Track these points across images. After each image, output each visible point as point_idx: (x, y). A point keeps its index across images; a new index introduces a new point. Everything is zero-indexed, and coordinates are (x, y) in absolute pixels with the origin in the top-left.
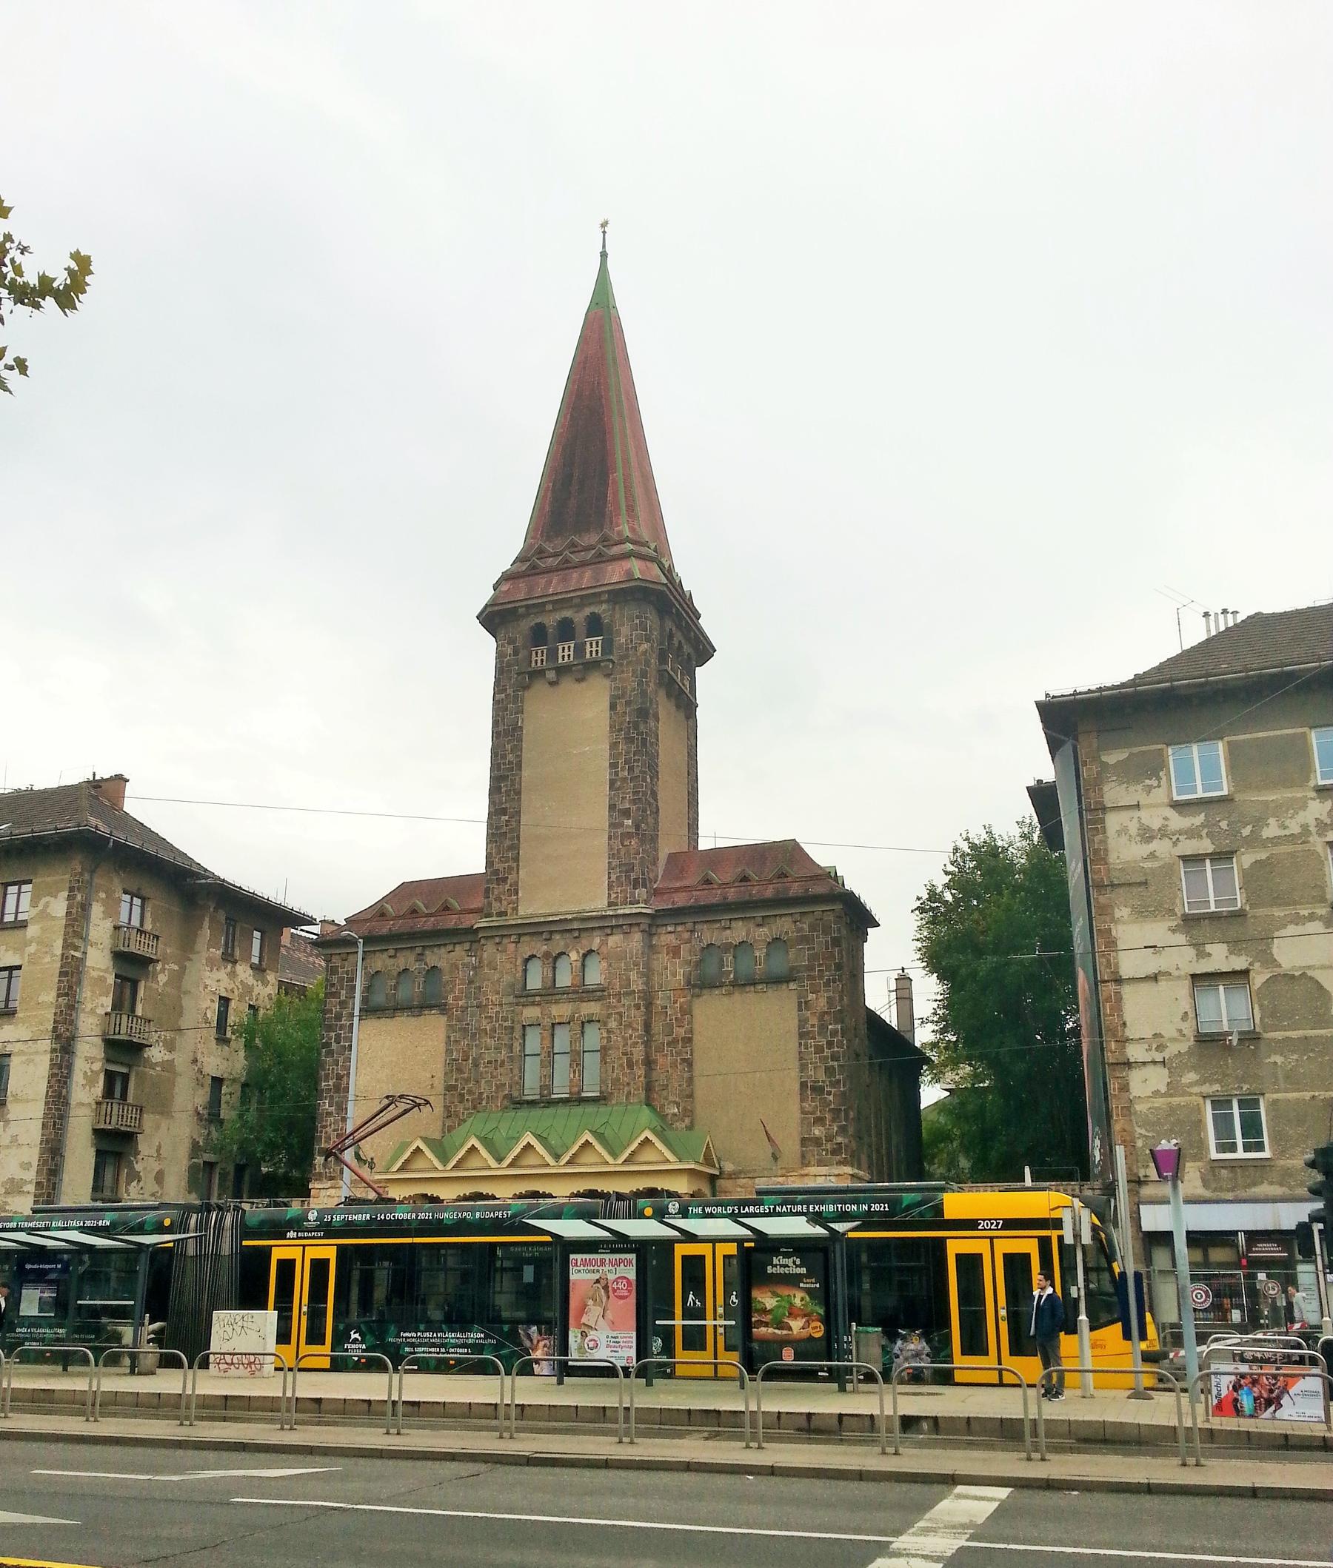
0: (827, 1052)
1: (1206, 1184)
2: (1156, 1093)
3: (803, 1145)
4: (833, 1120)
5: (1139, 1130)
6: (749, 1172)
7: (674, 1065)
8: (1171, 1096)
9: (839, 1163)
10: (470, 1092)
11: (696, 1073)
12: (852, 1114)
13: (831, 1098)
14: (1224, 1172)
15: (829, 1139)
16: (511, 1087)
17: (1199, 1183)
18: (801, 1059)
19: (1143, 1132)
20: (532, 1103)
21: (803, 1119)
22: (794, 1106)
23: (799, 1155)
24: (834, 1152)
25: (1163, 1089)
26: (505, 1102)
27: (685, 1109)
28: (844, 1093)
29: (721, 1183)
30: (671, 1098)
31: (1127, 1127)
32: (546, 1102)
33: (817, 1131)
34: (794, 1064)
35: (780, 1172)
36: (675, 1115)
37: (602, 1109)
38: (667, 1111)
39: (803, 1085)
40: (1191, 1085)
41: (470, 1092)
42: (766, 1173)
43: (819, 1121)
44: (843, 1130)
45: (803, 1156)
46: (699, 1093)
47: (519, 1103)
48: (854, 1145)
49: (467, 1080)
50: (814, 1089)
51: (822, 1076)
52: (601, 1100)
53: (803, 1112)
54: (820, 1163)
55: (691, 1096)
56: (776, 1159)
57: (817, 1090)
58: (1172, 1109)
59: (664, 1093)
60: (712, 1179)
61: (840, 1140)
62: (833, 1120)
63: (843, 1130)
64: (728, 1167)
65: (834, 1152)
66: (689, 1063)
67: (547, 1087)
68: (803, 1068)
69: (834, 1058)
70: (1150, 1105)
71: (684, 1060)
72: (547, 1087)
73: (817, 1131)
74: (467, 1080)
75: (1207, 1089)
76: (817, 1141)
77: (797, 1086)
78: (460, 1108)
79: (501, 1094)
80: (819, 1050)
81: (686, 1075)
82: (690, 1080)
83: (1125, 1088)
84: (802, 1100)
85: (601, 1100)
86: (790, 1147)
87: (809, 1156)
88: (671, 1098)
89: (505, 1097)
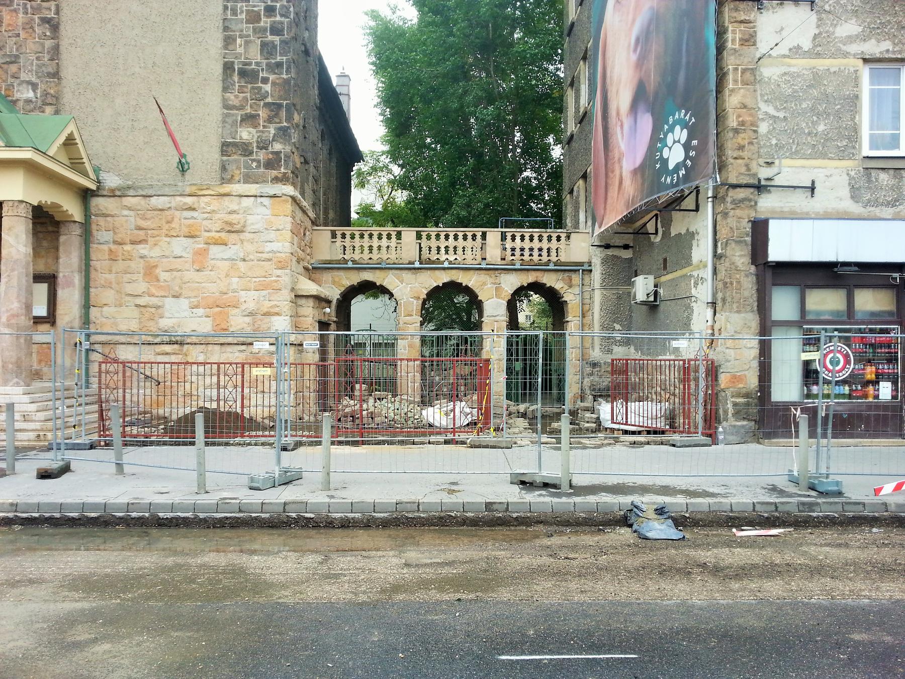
0: (265, 22)
1: (855, 194)
2: (796, 51)
3: (224, 153)
4: (270, 120)
5: (764, 107)
6: (142, 188)
7: (29, 26)
8: (818, 55)
9: (276, 180)
11: (64, 43)
12: (296, 118)
13: (268, 87)
14: (884, 177)
15: (263, 145)
17: (846, 192)
18: (226, 29)
19: (771, 110)
21: (226, 115)
22: (213, 96)
23: (217, 167)
24: (269, 165)
25: (807, 45)
27: (46, 94)
28: (287, 82)
29: (98, 203)
30: (24, 76)
31: (749, 102)
33: (246, 134)
34: (215, 40)
35: (188, 190)
36: (28, 101)
38: (17, 95)
39: (228, 67)
40: (851, 39)
42: (167, 191)
43: (250, 119)
44: (283, 133)
45: (224, 168)
46: (69, 71)
48: (298, 160)
50: (243, 73)
51: (255, 55)
53: (226, 106)
54: (248, 179)
56: (183, 171)
57: (247, 74)
58: (817, 78)
59: (13, 68)
60: (85, 195)
61: (277, 147)
62: (270, 120)
63: (283, 133)
64: (111, 181)
65: (269, 165)
66: (54, 26)
68: (228, 41)
69: (276, 30)
70: (787, 69)
71: (45, 21)
73: (246, 134)
75: (874, 48)
76: (245, 149)
77: (218, 69)
80: (254, 18)
81: (49, 43)
82: (56, 49)
83: (749, 40)
84: (225, 89)
86: (205, 155)
87: (231, 168)
88: (24, 76)
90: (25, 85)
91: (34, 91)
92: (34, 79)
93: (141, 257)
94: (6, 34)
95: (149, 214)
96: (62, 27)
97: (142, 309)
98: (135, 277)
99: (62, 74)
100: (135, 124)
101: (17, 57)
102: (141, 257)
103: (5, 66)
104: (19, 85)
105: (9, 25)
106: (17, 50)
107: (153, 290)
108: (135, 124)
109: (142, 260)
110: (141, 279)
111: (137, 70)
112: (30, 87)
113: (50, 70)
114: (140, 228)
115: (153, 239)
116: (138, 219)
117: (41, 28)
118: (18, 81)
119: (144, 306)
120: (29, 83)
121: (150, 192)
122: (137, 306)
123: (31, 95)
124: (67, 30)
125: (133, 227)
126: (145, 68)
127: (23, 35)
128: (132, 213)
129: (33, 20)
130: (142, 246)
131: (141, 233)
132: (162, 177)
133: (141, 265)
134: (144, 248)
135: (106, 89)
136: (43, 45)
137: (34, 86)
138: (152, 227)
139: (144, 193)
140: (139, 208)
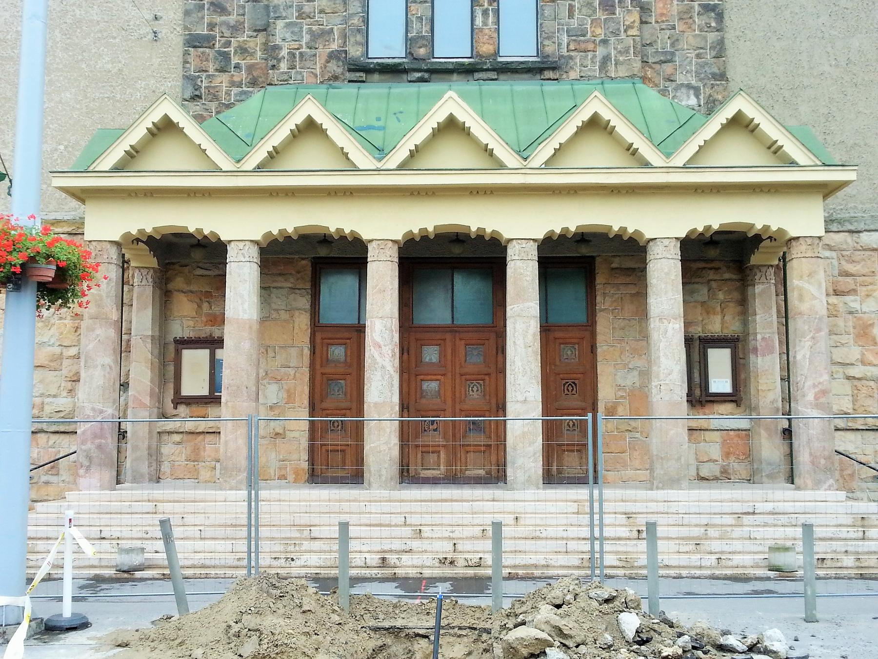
7: (685, 16)
10: (243, 50)
11: (730, 36)
16: (344, 36)
20: (391, 71)
26: (334, 67)
30: (681, 79)
32: (419, 68)
37: (550, 87)
41: (243, 50)
47: (364, 70)
49: (236, 29)
52: (541, 68)
55: (722, 76)
59: (668, 68)
67: (420, 38)
72: (420, 38)
74: (236, 29)
78: (222, 81)
79: (323, 51)
81: (712, 37)
82: (721, 43)
85: (541, 68)
88: (681, 79)
89: (332, 56)
90: (684, 90)
91: (697, 96)
92: (693, 82)
93: (851, 313)
94: (657, 26)
95: (858, 255)
96: (726, 17)
97: (856, 382)
98: (844, 339)
99: (729, 75)
100: (828, 138)
101: (673, 54)
102: (851, 313)
103: (657, 67)
104: (676, 89)
105: (662, 15)
106: (672, 45)
107: (870, 357)
108: (828, 138)
109: (850, 316)
110: (852, 341)
111: (826, 68)
112: (692, 92)
113: (716, 70)
114: (847, 274)
115: (864, 289)
116: (843, 262)
117: (704, 17)
118: (674, 85)
119: (859, 379)
120: (689, 86)
121: (861, 226)
122: (848, 378)
123: (693, 101)
124: (732, 20)
125: (836, 272)
126: (837, 66)
127: (680, 26)
128: (834, 254)
129: (692, 7)
130: (852, 298)
131: (849, 279)
132: (868, 206)
133: (850, 324)
134: (856, 301)
135: (787, 94)
136: (705, 38)
137: (697, 91)
138: (864, 271)
139: (852, 228)
140: (845, 247)
